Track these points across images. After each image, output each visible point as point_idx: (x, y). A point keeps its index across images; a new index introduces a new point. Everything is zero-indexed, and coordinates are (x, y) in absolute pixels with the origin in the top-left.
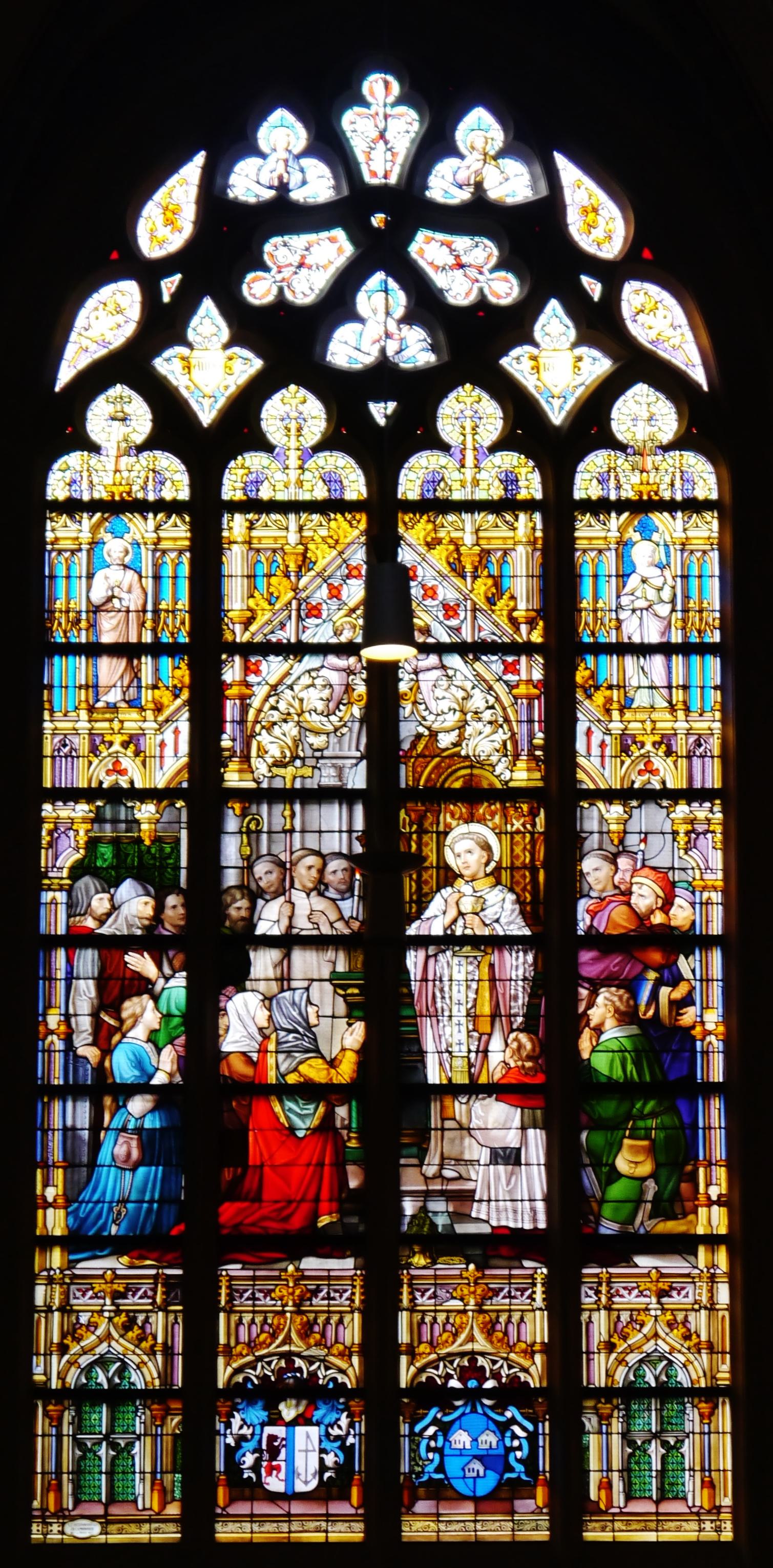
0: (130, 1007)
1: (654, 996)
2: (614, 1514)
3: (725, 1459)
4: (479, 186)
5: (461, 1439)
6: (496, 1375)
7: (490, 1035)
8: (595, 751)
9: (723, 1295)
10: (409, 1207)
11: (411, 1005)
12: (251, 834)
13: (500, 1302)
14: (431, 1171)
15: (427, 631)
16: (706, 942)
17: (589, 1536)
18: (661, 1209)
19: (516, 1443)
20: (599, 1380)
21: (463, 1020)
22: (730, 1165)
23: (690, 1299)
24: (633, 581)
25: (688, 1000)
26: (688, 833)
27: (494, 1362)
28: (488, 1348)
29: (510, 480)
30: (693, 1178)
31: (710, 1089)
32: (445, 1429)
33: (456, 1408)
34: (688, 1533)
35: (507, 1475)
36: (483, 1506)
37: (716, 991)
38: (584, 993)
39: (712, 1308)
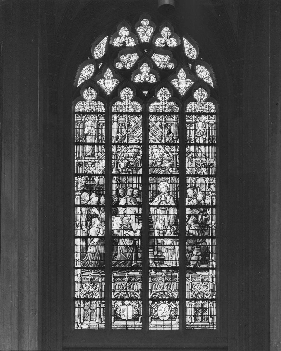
0: (94, 220)
2: (192, 324)
6: (168, 296)
7: (168, 226)
8: (189, 166)
11: (152, 220)
12: (118, 184)
14: (155, 254)
16: (212, 207)
18: (202, 263)
19: (172, 310)
21: (162, 223)
23: (208, 281)
26: (209, 184)
27: (168, 293)
28: (167, 291)
33: (160, 302)
35: (170, 316)
37: (214, 217)
38: (187, 217)
39: (212, 282)
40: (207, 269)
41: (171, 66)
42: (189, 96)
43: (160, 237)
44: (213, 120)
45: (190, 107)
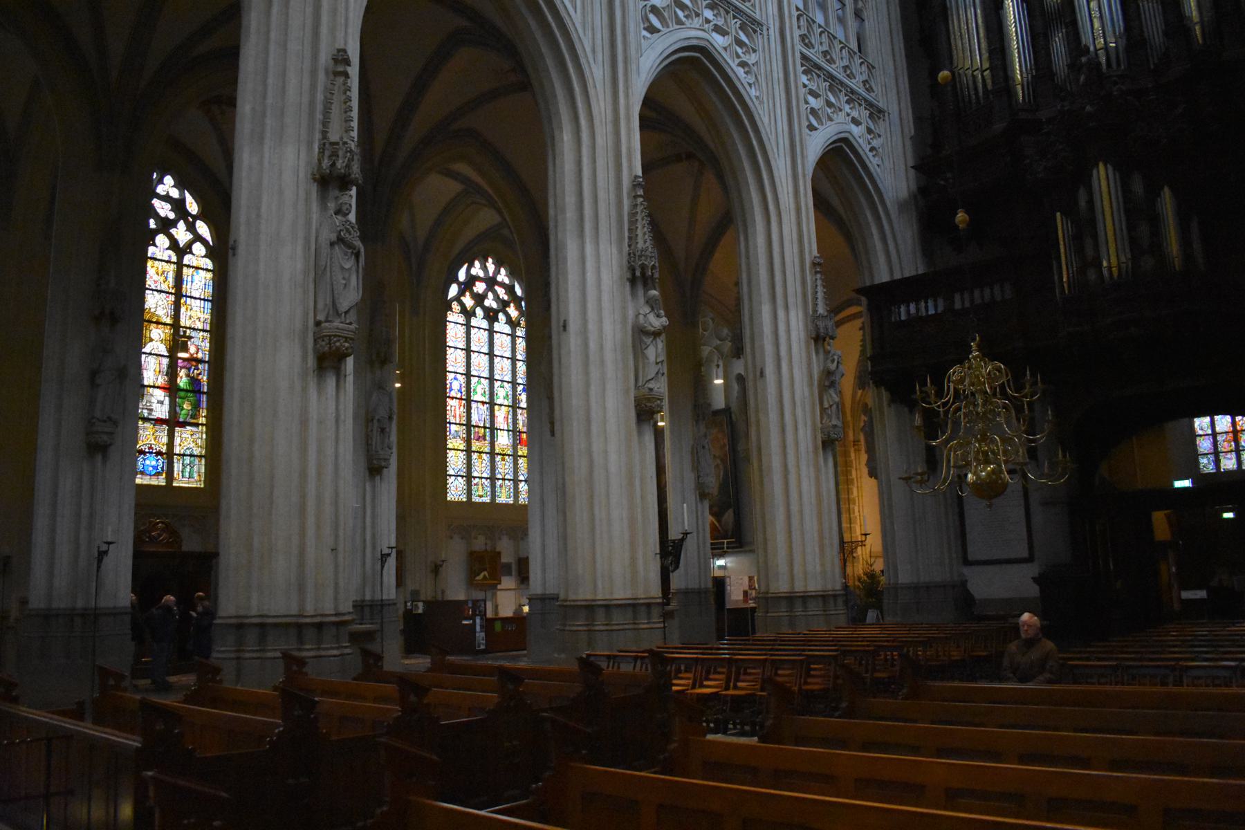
1: (193, 372)
3: (203, 470)
4: (168, 192)
5: (147, 462)
6: (156, 449)
9: (204, 436)
10: (140, 411)
13: (158, 434)
14: (144, 403)
15: (150, 286)
16: (205, 362)
17: (174, 485)
18: (192, 417)
20: (178, 452)
22: (207, 409)
24: (194, 284)
25: (200, 374)
29: (170, 257)
30: (199, 411)
31: (204, 393)
32: (145, 460)
34: (194, 485)
36: (152, 477)
37: (206, 372)
38: (179, 369)
39: (202, 439)
40: (197, 425)
41: (172, 216)
42: (188, 249)
43: (150, 387)
44: (210, 275)
45: (187, 259)
